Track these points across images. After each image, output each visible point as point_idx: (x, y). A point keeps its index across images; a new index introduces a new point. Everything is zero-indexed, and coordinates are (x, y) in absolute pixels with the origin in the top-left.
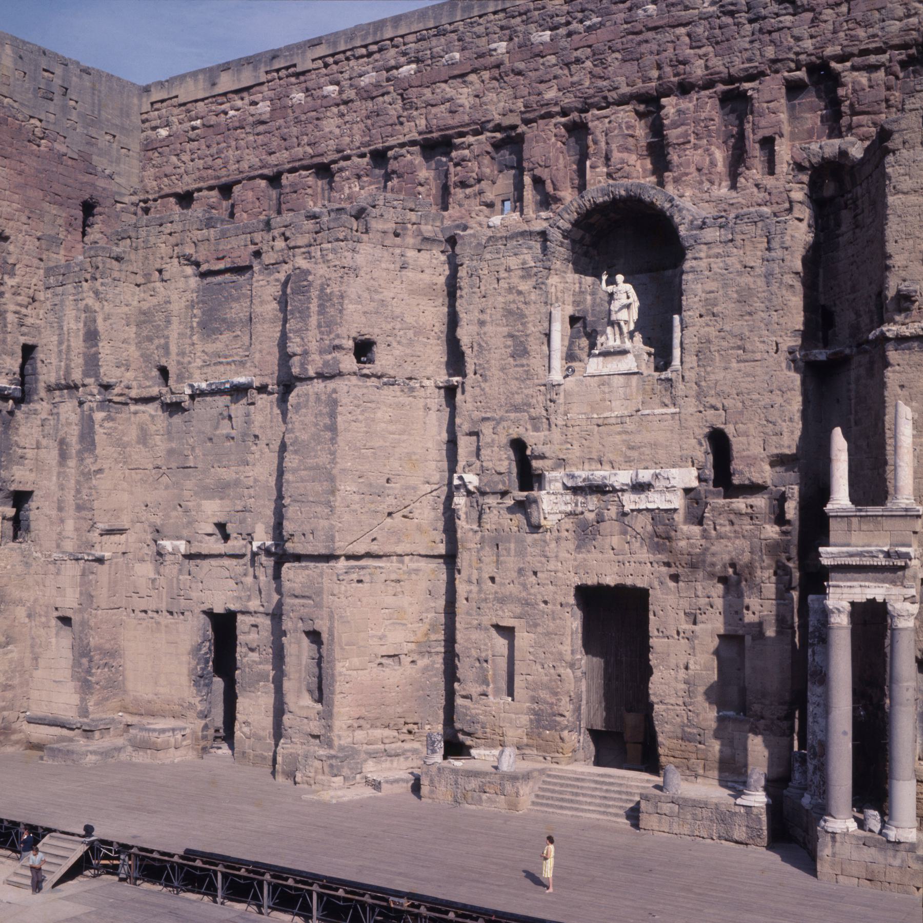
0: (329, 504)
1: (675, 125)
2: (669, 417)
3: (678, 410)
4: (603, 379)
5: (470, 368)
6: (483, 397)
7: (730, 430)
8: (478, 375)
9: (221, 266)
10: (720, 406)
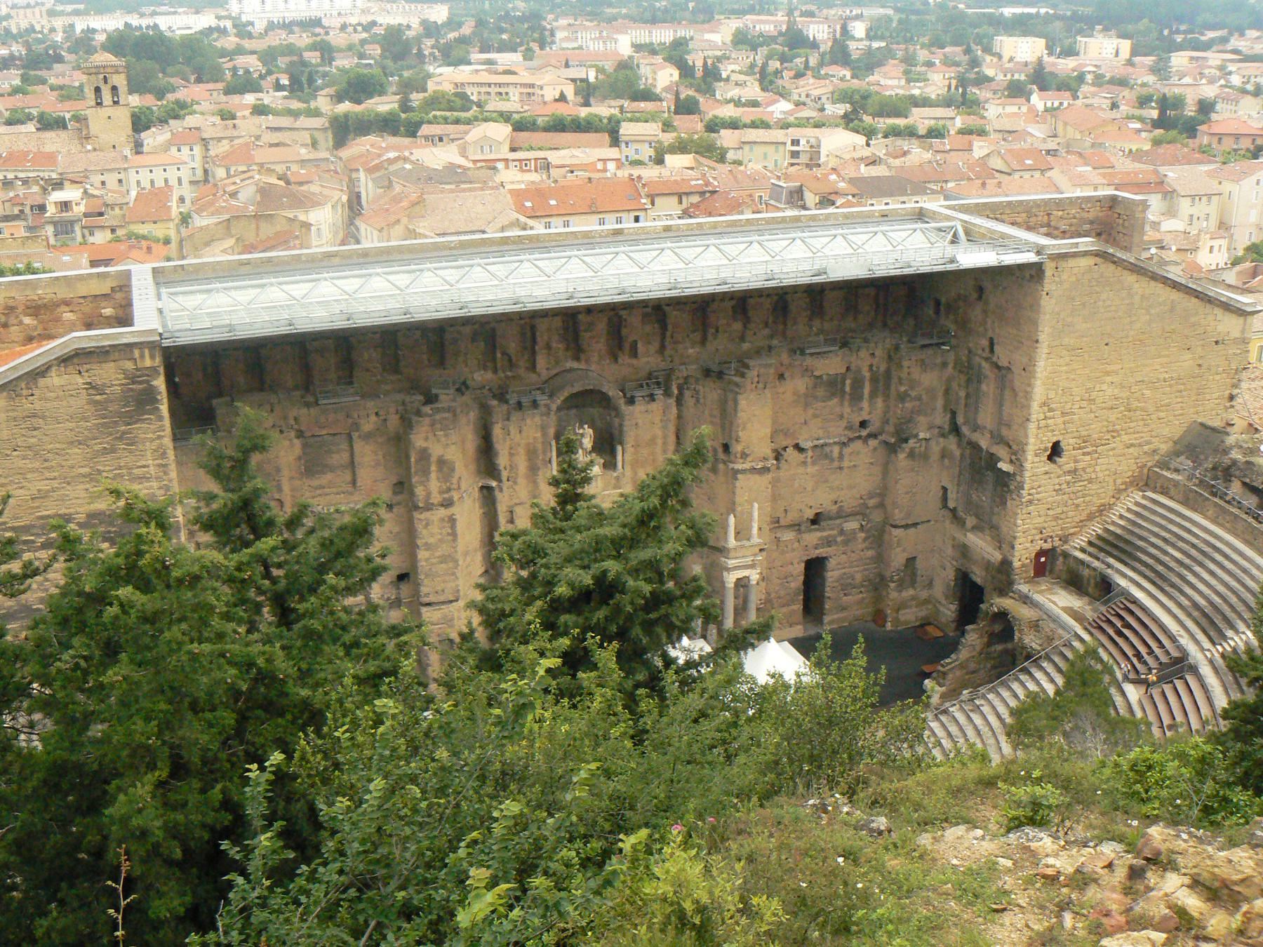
0: (454, 574)
1: (586, 331)
9: (324, 432)
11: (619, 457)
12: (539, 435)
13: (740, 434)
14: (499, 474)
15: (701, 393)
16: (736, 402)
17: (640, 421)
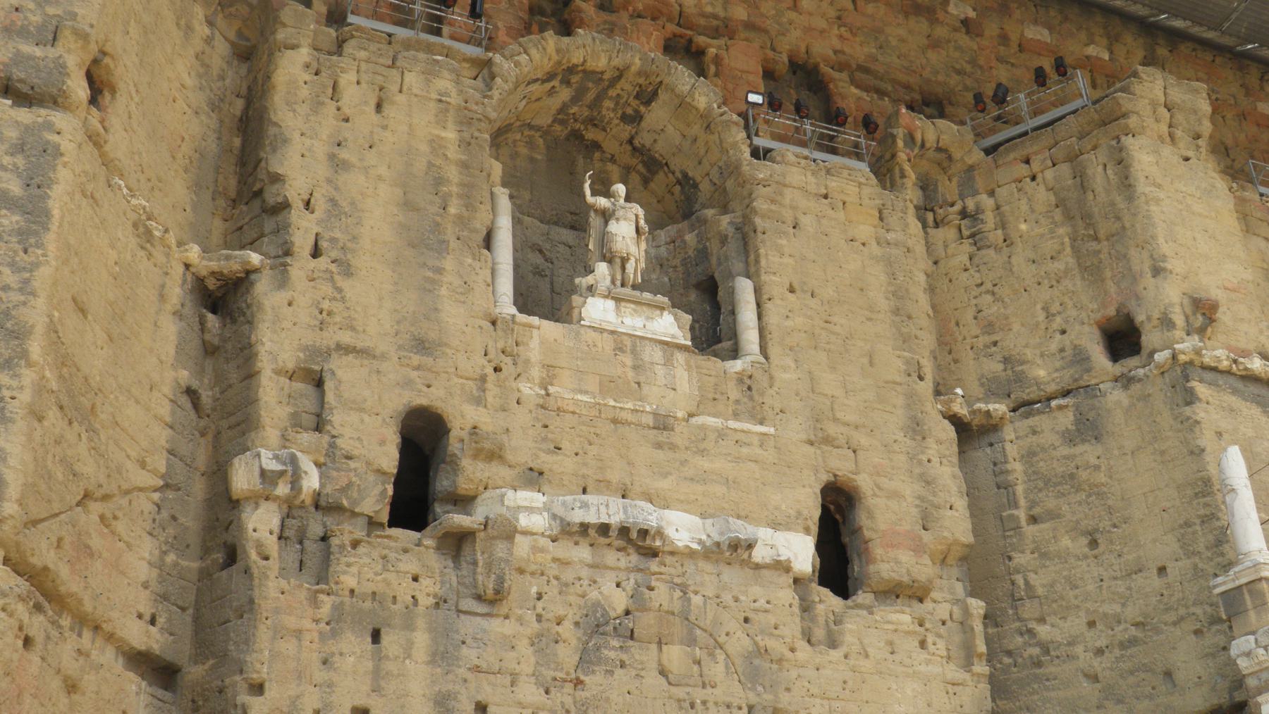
2: (756, 440)
3: (772, 430)
4: (624, 343)
5: (302, 242)
6: (337, 307)
7: (864, 482)
8: (323, 262)
10: (842, 441)
11: (747, 316)
12: (451, 135)
13: (1165, 248)
14: (282, 229)
15: (989, 218)
16: (1121, 161)
17: (806, 221)
